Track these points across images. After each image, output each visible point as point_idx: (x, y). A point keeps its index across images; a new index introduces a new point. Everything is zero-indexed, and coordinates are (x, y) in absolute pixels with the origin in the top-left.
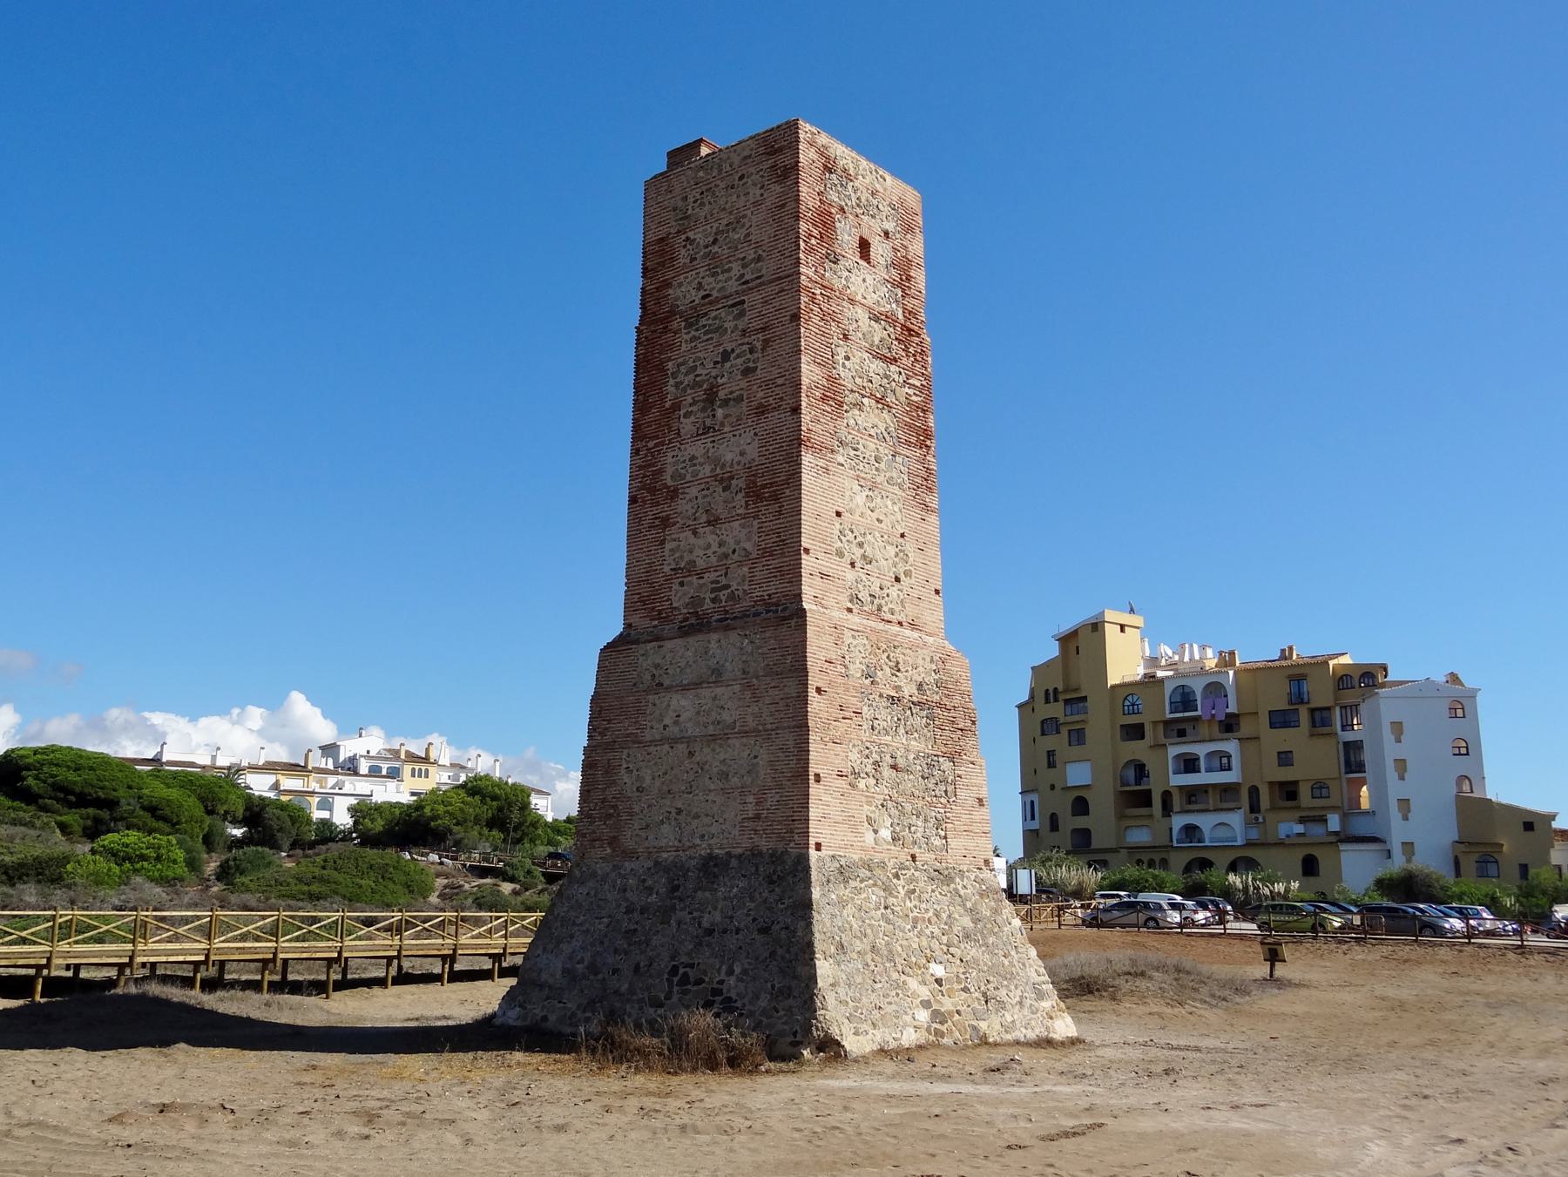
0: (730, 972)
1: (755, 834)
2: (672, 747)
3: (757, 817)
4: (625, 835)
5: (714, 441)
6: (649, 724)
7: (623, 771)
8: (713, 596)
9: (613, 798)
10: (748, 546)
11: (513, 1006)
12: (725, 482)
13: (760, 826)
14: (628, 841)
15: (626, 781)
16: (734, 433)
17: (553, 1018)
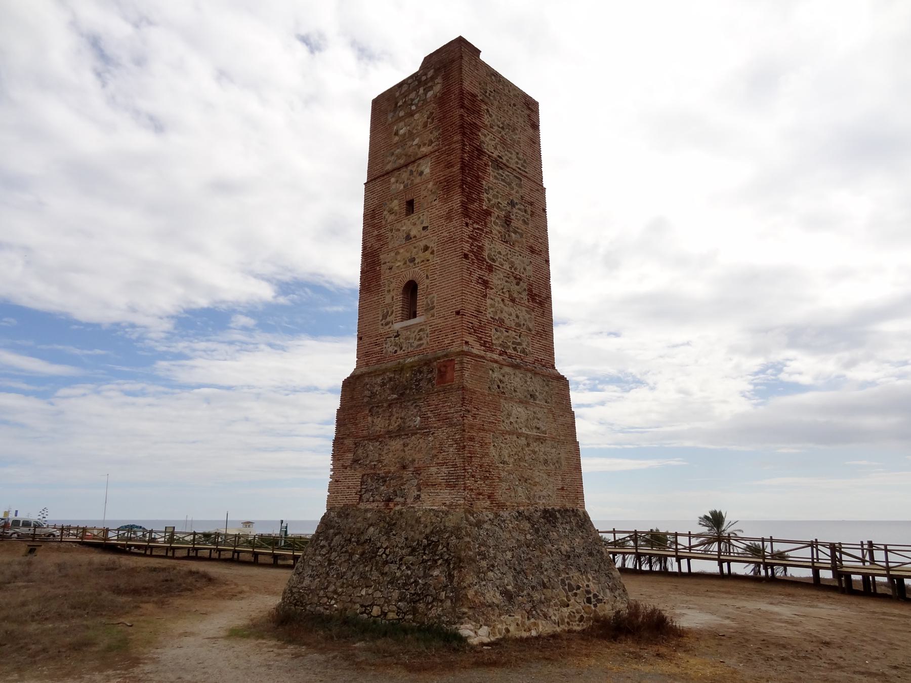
0: (589, 580)
1: (563, 498)
2: (518, 438)
3: (562, 489)
4: (498, 493)
5: (510, 251)
6: (502, 419)
7: (492, 448)
8: (514, 346)
9: (487, 465)
10: (531, 326)
11: (479, 625)
12: (519, 280)
13: (564, 493)
14: (500, 495)
15: (495, 455)
16: (521, 254)
17: (512, 629)
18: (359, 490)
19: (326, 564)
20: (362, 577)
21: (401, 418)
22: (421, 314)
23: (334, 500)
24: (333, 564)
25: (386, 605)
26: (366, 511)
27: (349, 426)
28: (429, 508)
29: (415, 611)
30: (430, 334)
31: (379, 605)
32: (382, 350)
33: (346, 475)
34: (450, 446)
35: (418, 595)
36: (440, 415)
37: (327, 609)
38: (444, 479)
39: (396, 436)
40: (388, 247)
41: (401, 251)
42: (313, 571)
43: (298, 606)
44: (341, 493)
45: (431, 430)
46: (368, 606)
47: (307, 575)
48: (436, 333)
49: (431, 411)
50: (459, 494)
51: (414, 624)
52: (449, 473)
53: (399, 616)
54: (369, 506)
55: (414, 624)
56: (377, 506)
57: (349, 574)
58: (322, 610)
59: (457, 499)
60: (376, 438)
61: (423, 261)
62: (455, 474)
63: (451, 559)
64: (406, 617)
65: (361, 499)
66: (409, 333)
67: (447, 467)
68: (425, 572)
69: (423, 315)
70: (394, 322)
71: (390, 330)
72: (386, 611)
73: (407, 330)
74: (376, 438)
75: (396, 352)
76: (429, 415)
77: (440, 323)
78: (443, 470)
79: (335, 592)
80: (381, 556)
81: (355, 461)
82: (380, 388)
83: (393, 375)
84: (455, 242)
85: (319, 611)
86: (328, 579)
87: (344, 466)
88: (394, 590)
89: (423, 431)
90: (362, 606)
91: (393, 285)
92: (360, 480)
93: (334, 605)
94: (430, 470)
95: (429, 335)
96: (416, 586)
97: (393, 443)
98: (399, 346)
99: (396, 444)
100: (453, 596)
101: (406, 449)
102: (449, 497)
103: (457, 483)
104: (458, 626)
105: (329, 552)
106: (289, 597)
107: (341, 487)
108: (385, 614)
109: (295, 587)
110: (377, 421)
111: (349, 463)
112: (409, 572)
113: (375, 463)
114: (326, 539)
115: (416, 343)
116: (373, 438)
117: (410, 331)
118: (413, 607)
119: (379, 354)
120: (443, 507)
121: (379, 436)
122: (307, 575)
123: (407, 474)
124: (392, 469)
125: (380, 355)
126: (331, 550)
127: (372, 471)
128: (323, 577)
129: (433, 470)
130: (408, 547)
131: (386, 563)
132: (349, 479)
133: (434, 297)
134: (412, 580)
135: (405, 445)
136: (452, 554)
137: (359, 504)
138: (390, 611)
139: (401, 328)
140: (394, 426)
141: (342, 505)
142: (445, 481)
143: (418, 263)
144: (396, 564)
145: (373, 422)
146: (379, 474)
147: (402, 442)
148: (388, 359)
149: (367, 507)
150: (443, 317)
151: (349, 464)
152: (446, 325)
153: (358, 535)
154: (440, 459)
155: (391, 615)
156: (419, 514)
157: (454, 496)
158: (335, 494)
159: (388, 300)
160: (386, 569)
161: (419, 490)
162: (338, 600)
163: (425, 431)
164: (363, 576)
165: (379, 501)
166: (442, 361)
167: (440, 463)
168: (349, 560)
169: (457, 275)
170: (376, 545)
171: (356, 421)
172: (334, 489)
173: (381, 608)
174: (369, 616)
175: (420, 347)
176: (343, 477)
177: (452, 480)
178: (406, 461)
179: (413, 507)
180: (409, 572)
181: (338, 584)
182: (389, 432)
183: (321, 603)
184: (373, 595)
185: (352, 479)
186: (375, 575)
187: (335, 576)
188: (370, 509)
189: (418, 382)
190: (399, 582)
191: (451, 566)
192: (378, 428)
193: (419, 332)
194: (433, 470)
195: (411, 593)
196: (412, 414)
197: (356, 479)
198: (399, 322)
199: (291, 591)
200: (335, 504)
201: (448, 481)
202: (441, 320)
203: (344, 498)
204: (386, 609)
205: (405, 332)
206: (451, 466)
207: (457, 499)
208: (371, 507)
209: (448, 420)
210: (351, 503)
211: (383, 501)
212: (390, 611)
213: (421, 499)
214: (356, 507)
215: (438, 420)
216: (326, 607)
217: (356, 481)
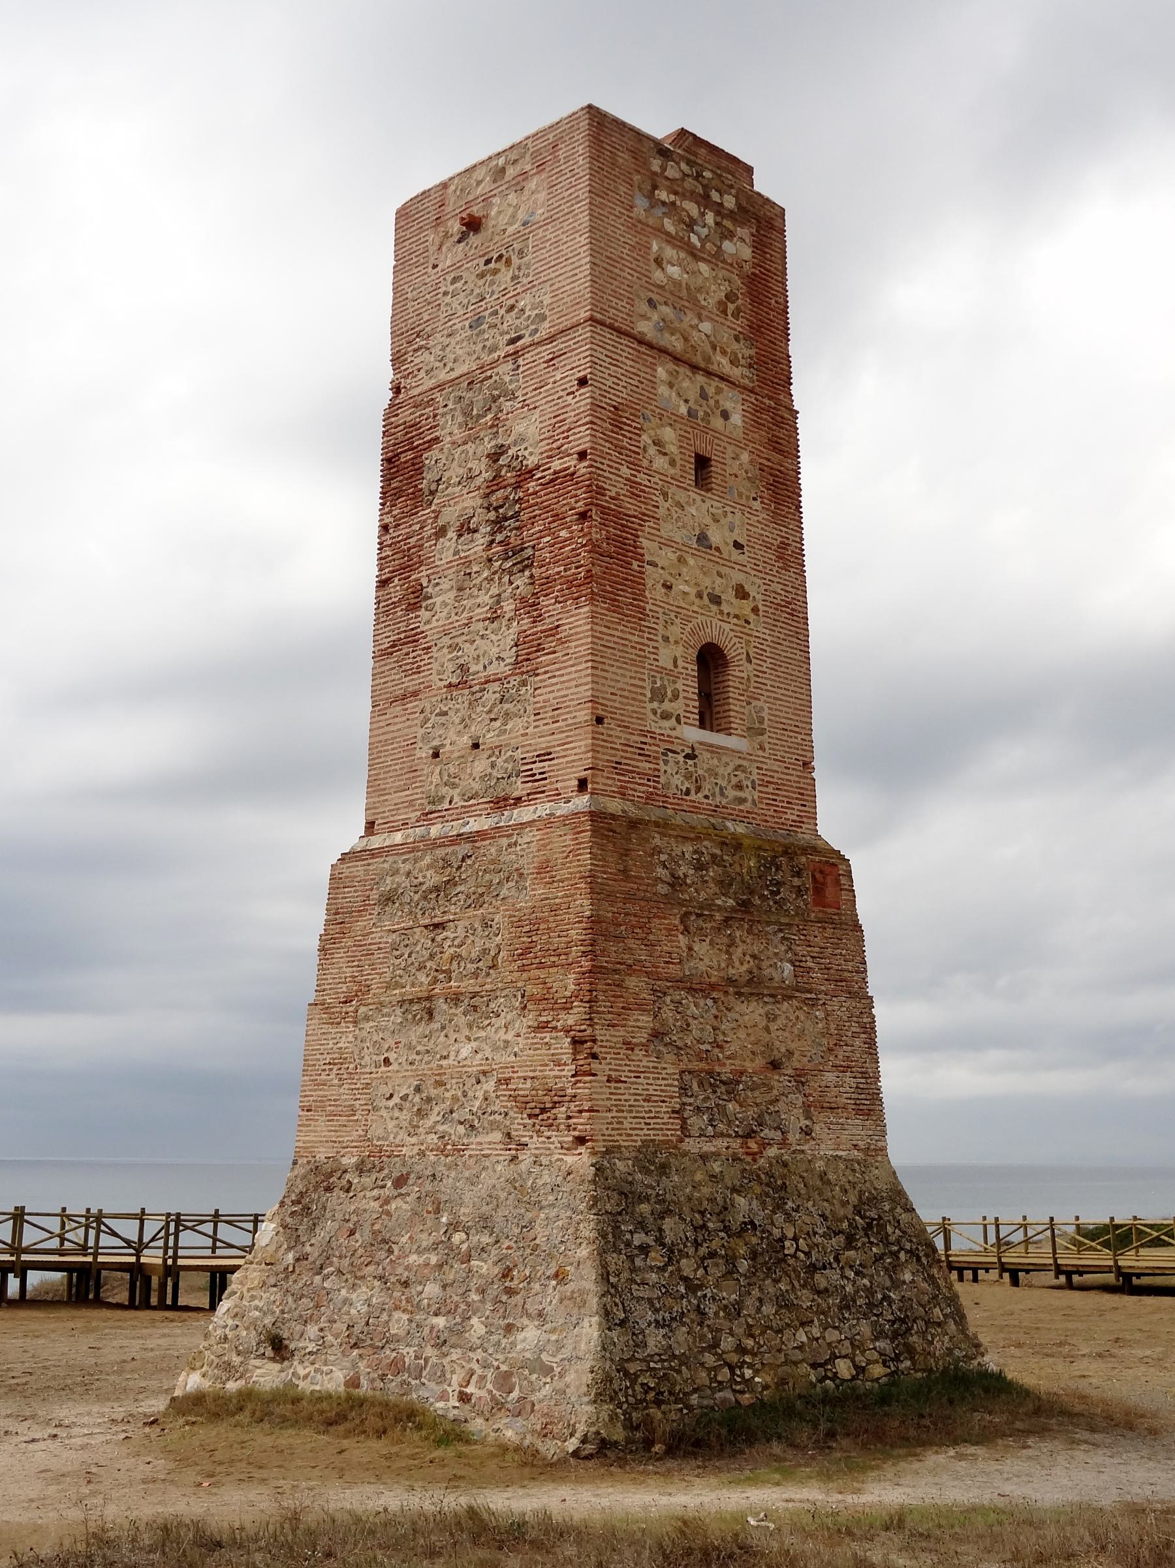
18: (678, 1106)
19: (682, 1289)
20: (781, 1307)
21: (754, 957)
22: (739, 732)
23: (613, 1129)
24: (700, 1287)
25: (858, 1352)
26: (704, 1157)
27: (631, 943)
28: (831, 1153)
29: (910, 1351)
30: (760, 785)
31: (845, 1357)
32: (656, 773)
33: (639, 1066)
34: (854, 1035)
35: (902, 1321)
36: (828, 969)
37: (742, 1392)
38: (850, 1099)
39: (752, 994)
40: (659, 530)
41: (691, 561)
42: (657, 1311)
43: (663, 1402)
44: (631, 1111)
45: (820, 996)
46: (826, 1362)
47: (649, 1325)
48: (770, 789)
49: (812, 957)
50: (879, 1128)
51: (919, 1375)
52: (857, 1087)
53: (889, 1367)
54: (708, 1148)
55: (919, 1375)
56: (727, 1148)
57: (750, 1303)
58: (728, 1394)
59: (877, 1138)
60: (698, 988)
61: (736, 616)
62: (867, 1091)
63: (917, 1249)
64: (902, 1366)
65: (684, 1128)
66: (715, 761)
67: (853, 1075)
68: (891, 1277)
69: (745, 737)
70: (683, 720)
71: (673, 733)
72: (864, 1364)
73: (712, 752)
74: (698, 988)
75: (688, 793)
76: (810, 964)
77: (778, 772)
78: (847, 1080)
79: (741, 1350)
80: (794, 1256)
81: (656, 1035)
82: (691, 872)
83: (718, 852)
84: (796, 619)
85: (724, 1400)
86: (707, 1322)
87: (629, 1043)
88: (858, 1319)
89: (804, 996)
90: (814, 1366)
91: (674, 631)
92: (676, 1083)
93: (753, 1378)
94: (824, 1078)
95: (758, 788)
96: (890, 1305)
97: (741, 1007)
98: (697, 781)
99: (752, 1012)
100: (952, 1313)
101: (773, 1027)
102: (862, 1133)
103: (872, 1107)
104: (979, 1359)
105: (670, 1259)
106: (627, 1388)
107: (626, 1097)
108: (863, 1369)
109: (632, 1359)
110: (701, 948)
111: (642, 1037)
112: (866, 1281)
113: (708, 1047)
114: (641, 1226)
115: (732, 793)
116: (698, 987)
117: (719, 760)
118: (904, 1344)
119: (649, 780)
120: (856, 1152)
121: (713, 987)
122: (649, 1325)
123: (780, 1081)
124: (749, 1066)
125: (651, 783)
126: (672, 1254)
127: (703, 1065)
128: (693, 1321)
129: (830, 1077)
130: (836, 1234)
131: (813, 1269)
132: (649, 1078)
133: (762, 708)
134: (880, 1296)
135: (771, 1017)
136: (914, 1240)
137: (682, 1141)
138: (869, 1362)
139: (701, 743)
140: (740, 970)
141: (639, 1143)
142: (853, 1102)
143: (728, 614)
144: (832, 1268)
145: (690, 949)
146: (719, 1074)
147: (762, 1011)
148: (671, 800)
149: (705, 1149)
150: (781, 761)
151: (644, 1041)
152: (787, 780)
153: (718, 1215)
154: (840, 1057)
155: (877, 1370)
156: (820, 1165)
157: (871, 1133)
158: (615, 1114)
159: (665, 661)
160: (820, 1280)
161: (808, 1117)
162: (758, 1366)
163: (809, 996)
164: (784, 1303)
165: (729, 1136)
166: (817, 859)
167: (841, 1066)
168: (730, 1273)
169: (790, 685)
170: (771, 1234)
171: (651, 937)
172: (608, 1099)
173: (853, 1361)
174: (838, 1381)
175: (740, 803)
176: (630, 1071)
177: (863, 1102)
178: (776, 1052)
179: (803, 1152)
180: (866, 1281)
181: (739, 1331)
182: (731, 981)
183: (720, 1383)
184: (824, 1338)
185: (654, 1079)
186: (805, 1298)
187: (722, 1314)
188: (713, 1153)
189: (775, 885)
190: (858, 1303)
191: (924, 1260)
192: (702, 967)
193: (736, 770)
194: (830, 1077)
195: (889, 1321)
196: (776, 954)
197: (663, 1079)
198: (691, 725)
199: (627, 1374)
200: (618, 1138)
201: (858, 1102)
202: (779, 766)
203: (643, 1126)
204: (861, 1360)
205: (709, 755)
206: (860, 1075)
207: (877, 1138)
208: (713, 1149)
209: (844, 984)
210: (661, 1138)
211: (737, 1135)
212: (869, 1362)
213: (813, 1135)
214: (675, 1147)
215: (826, 980)
216: (738, 1387)
217: (665, 1085)
